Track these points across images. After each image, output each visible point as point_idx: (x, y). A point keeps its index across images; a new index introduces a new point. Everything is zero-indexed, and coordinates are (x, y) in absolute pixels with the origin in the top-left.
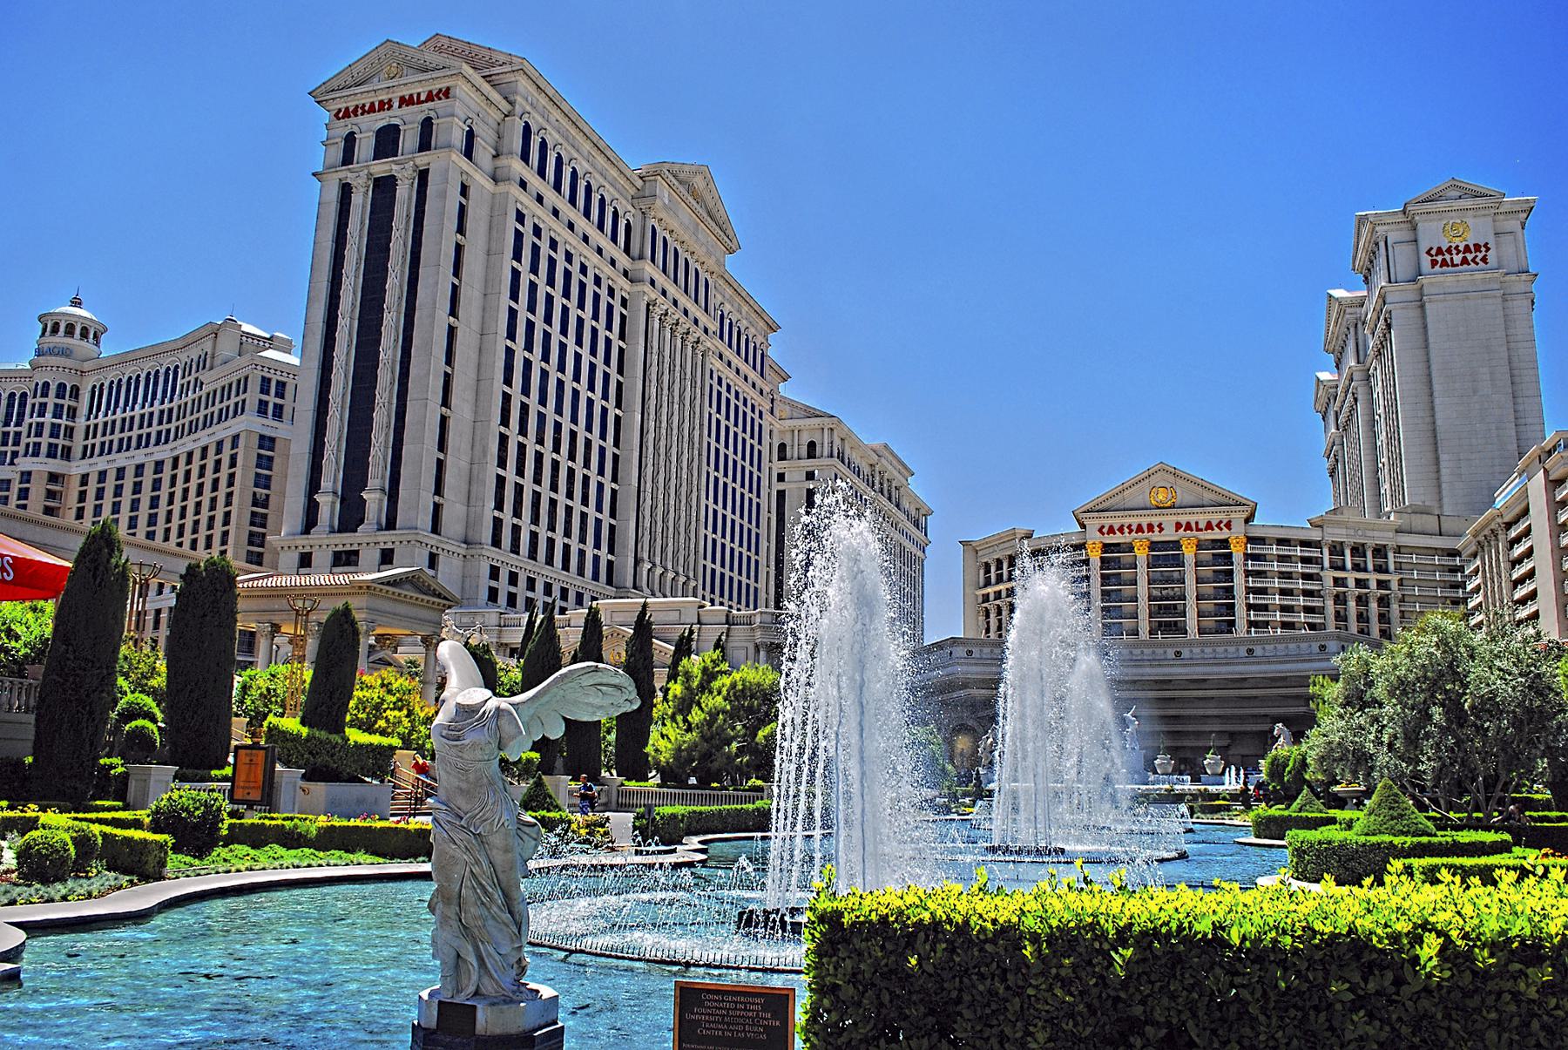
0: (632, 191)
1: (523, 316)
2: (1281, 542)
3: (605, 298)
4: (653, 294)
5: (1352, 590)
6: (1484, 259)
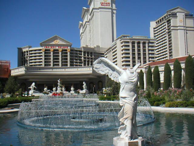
2: (77, 51)
6: (109, 5)
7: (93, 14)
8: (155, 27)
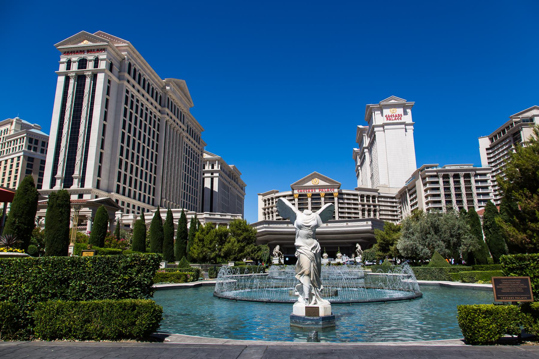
0: (162, 86)
1: (128, 122)
3: (153, 118)
4: (168, 118)
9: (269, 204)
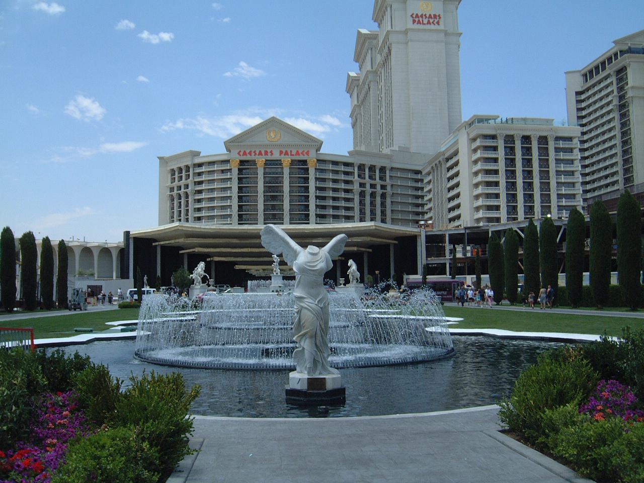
2: (335, 163)
5: (368, 190)
6: (438, 23)
7: (390, 51)
8: (580, 89)
9: (181, 178)
